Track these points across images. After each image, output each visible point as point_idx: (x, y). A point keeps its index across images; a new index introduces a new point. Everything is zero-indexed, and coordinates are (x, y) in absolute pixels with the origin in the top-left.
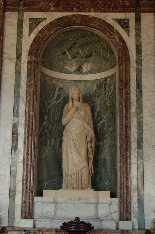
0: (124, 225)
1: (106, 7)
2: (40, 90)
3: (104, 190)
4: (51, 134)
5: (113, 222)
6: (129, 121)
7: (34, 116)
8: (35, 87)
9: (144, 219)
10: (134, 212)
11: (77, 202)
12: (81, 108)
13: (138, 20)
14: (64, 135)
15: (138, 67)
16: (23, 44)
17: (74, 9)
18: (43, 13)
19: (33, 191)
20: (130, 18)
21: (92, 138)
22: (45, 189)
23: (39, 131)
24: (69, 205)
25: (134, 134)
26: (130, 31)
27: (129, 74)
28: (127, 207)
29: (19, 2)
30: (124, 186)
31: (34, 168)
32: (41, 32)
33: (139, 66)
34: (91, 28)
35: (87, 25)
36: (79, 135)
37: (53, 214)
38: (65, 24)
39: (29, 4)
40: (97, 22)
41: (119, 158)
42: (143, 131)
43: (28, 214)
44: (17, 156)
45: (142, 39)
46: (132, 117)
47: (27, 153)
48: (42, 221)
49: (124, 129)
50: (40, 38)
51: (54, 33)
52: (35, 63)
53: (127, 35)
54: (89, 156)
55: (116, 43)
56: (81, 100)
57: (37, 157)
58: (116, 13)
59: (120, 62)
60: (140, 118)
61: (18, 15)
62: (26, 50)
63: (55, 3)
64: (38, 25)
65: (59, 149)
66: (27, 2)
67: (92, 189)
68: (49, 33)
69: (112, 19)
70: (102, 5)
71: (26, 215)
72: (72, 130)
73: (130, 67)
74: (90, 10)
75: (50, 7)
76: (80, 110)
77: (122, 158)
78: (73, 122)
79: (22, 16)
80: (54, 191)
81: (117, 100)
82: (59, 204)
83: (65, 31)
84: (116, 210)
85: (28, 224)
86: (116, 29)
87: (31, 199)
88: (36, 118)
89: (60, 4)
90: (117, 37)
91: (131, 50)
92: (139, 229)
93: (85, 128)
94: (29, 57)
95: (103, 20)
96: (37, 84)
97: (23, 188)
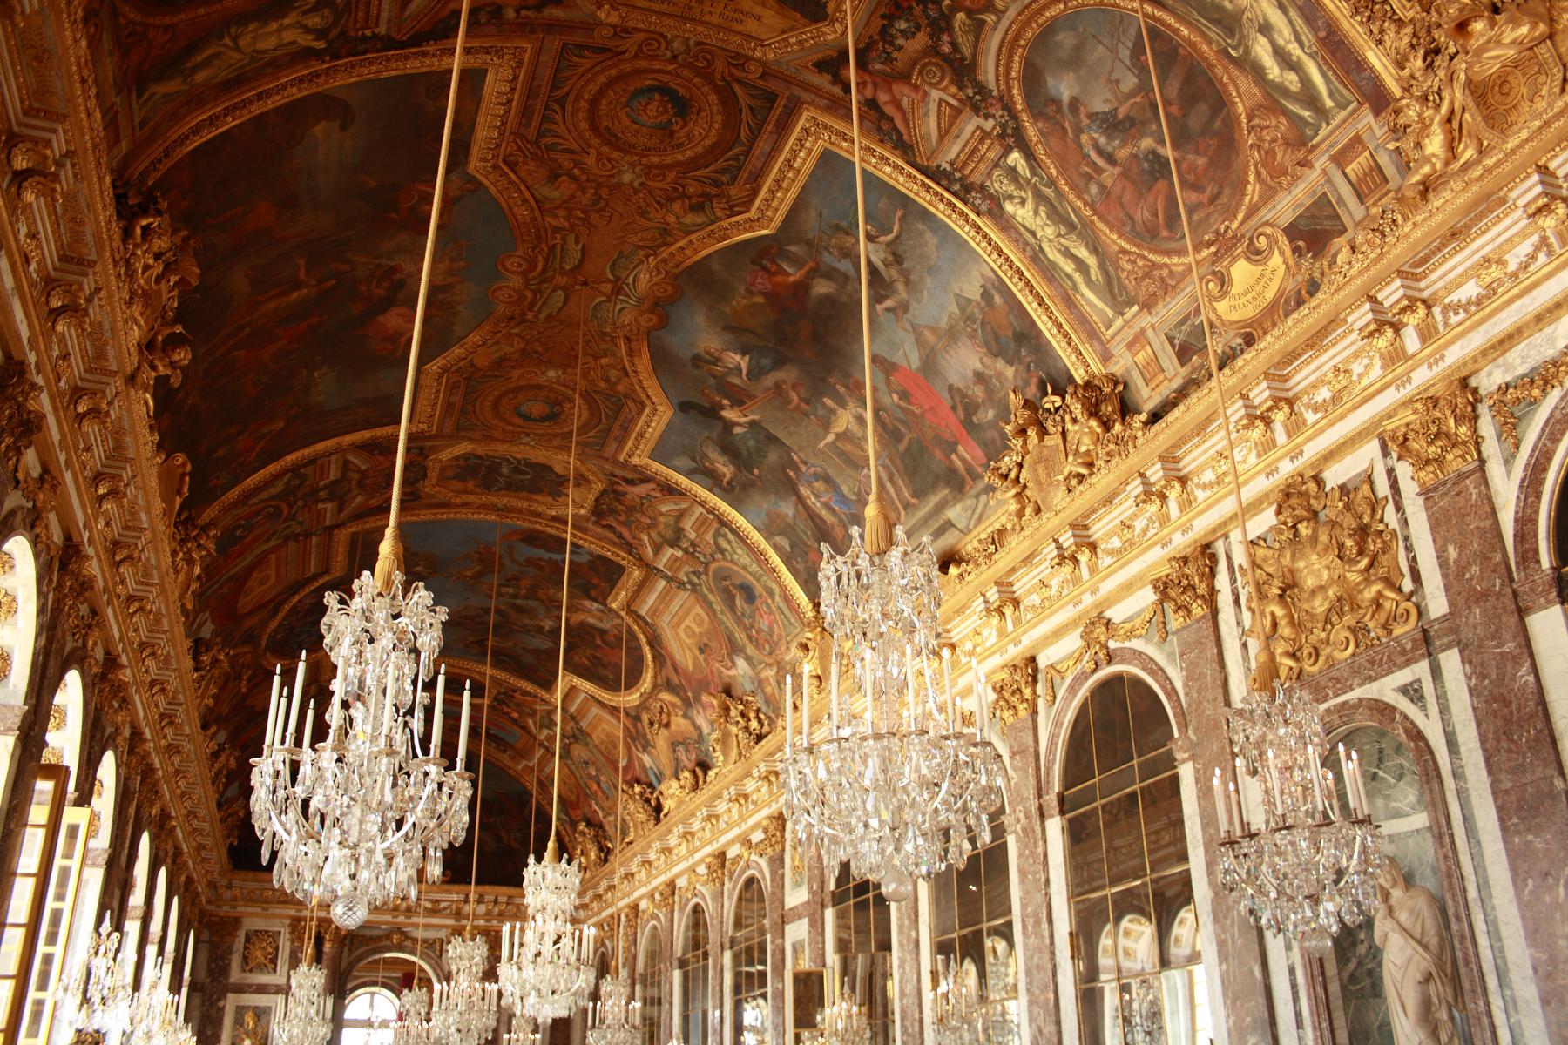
13: (1436, 672)
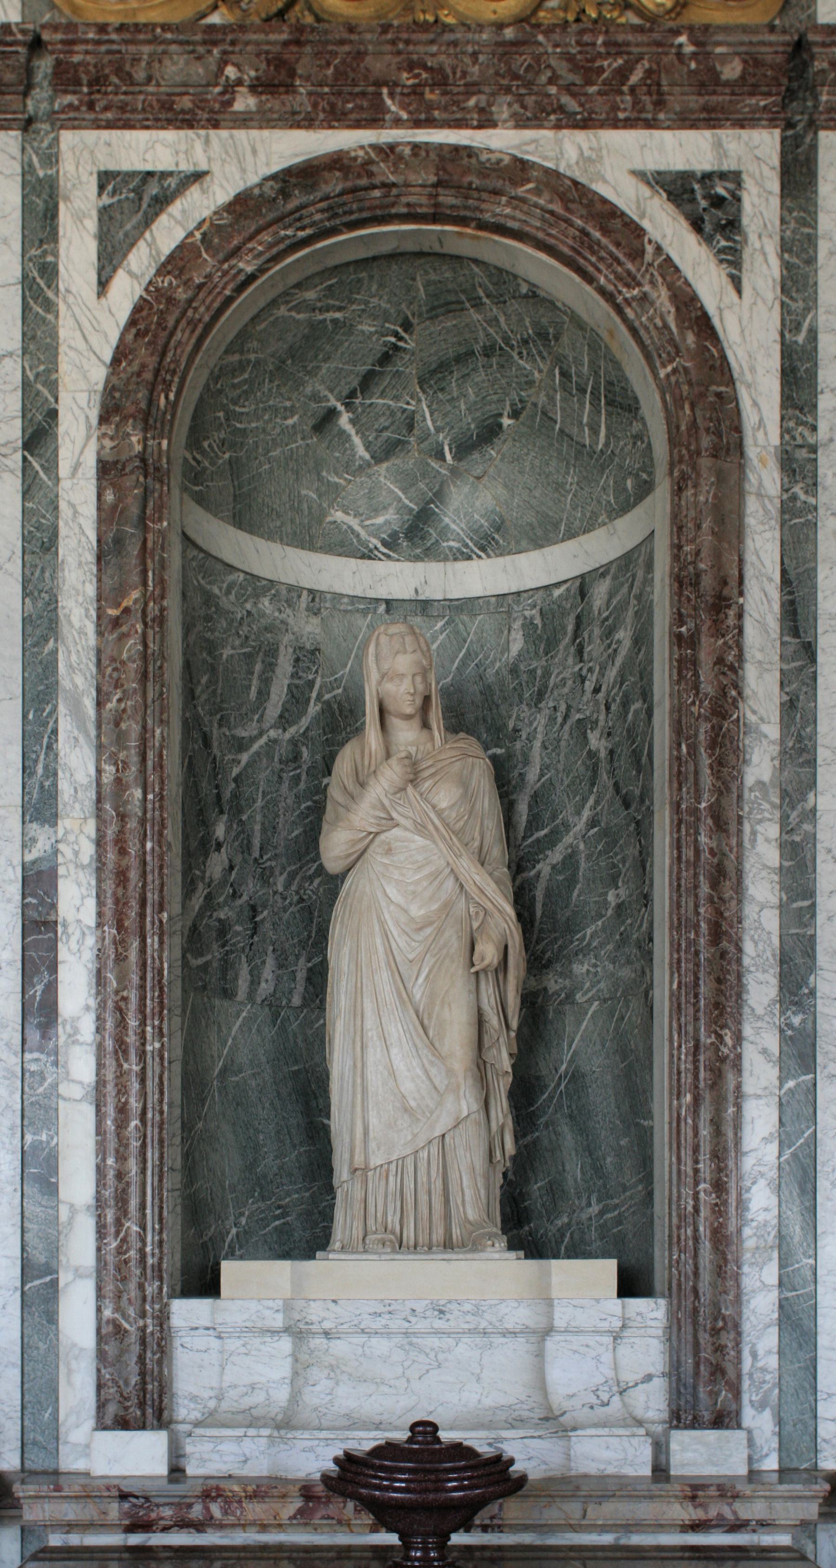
0: (699, 1454)
1: (592, 89)
2: (184, 654)
3: (576, 1252)
4: (255, 931)
5: (634, 1435)
6: (734, 842)
7: (149, 815)
8: (150, 632)
9: (816, 1417)
10: (757, 1376)
11: (421, 1325)
12: (440, 765)
13: (797, 175)
14: (336, 931)
15: (794, 498)
16: (62, 349)
17: (382, 101)
18: (182, 133)
19: (160, 1270)
20: (749, 168)
21: (506, 947)
22: (231, 1255)
23: (183, 907)
24: (380, 1346)
25: (763, 920)
26: (746, 256)
27: (734, 541)
28: (719, 1349)
29: (29, 61)
30: (701, 1229)
31: (160, 1133)
32: (177, 262)
33: (797, 489)
34: (496, 238)
35: (468, 214)
36: (428, 931)
37: (282, 1395)
38: (330, 208)
39: (91, 68)
40: (537, 192)
41: (671, 1062)
42: (819, 900)
43: (139, 1397)
44: (56, 1063)
45: (821, 311)
46: (750, 813)
47: (115, 1047)
48: (221, 1439)
49: (705, 889)
50: (170, 300)
51: (262, 270)
52: (146, 477)
53: (725, 280)
54: (490, 1056)
55: (654, 333)
56: (436, 716)
57: (177, 1068)
58: (656, 133)
59: (681, 461)
60: (801, 822)
61: (23, 149)
62: (83, 385)
63: (263, 66)
64: (153, 221)
65: (305, 1017)
66: (76, 59)
67: (511, 1247)
68: (225, 273)
69: (634, 173)
70: (571, 77)
71: (126, 1409)
72: (383, 904)
73: (741, 494)
74: (491, 113)
75: (230, 88)
76: (433, 775)
77: (690, 1066)
78: (389, 851)
79: (49, 157)
80: (284, 1267)
81: (656, 712)
82: (318, 1342)
83: (331, 262)
84: (652, 1370)
85: (138, 1456)
86: (659, 240)
87: (149, 1314)
88: (163, 826)
89: (292, 74)
90: (664, 293)
91: (749, 386)
92: (784, 1473)
93: (462, 886)
94: (104, 435)
95: (576, 183)
96: (162, 610)
97: (99, 1249)
